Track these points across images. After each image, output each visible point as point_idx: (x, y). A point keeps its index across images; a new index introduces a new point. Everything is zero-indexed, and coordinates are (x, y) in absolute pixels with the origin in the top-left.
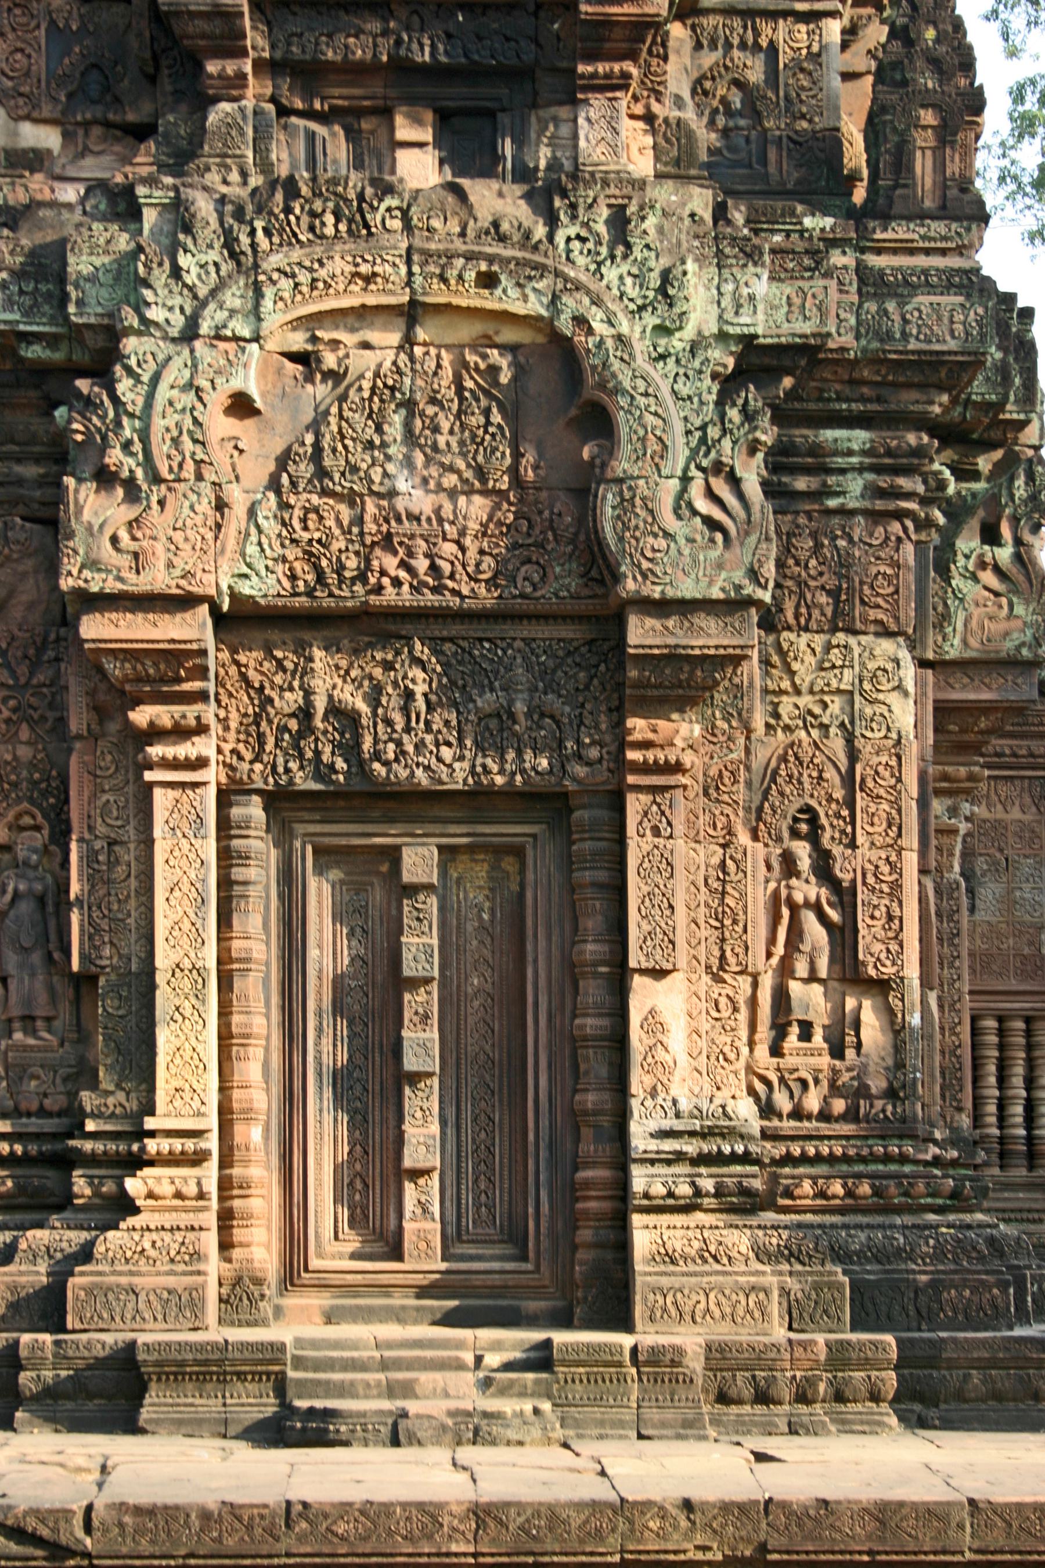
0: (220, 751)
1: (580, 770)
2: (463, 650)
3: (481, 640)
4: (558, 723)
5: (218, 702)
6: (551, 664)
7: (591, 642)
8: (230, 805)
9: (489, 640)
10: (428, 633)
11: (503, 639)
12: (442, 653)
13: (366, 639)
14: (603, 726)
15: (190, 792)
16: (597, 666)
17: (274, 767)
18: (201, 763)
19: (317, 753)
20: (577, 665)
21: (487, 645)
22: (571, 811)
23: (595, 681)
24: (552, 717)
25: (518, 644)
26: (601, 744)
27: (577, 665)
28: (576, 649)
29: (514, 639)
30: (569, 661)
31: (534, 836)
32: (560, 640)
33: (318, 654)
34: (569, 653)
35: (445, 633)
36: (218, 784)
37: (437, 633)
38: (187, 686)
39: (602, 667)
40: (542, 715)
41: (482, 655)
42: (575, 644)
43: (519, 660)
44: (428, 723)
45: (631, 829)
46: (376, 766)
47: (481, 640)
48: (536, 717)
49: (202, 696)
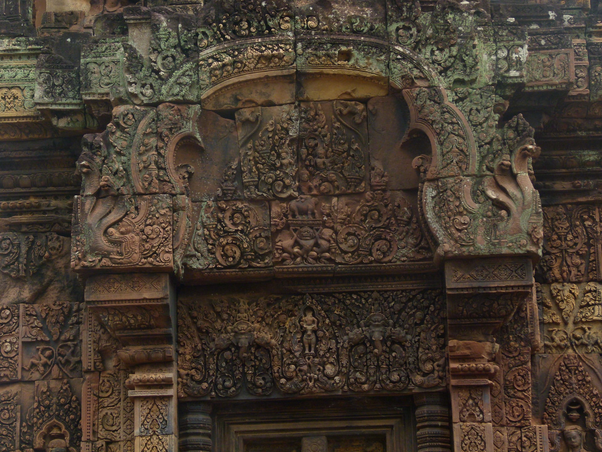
0: (179, 375)
1: (419, 378)
2: (339, 300)
3: (351, 293)
4: (403, 346)
5: (178, 342)
6: (398, 307)
7: (423, 292)
8: (187, 412)
9: (356, 293)
10: (316, 290)
11: (365, 292)
12: (325, 303)
13: (275, 296)
14: (434, 347)
15: (158, 403)
16: (428, 307)
17: (216, 384)
18: (167, 384)
19: (244, 374)
20: (415, 307)
21: (355, 297)
22: (416, 408)
23: (427, 317)
24: (400, 343)
25: (375, 295)
26: (432, 360)
27: (415, 307)
28: (414, 296)
29: (372, 292)
30: (410, 304)
31: (391, 427)
32: (403, 291)
33: (243, 306)
34: (410, 300)
35: (326, 290)
36: (179, 398)
37: (321, 290)
38: (156, 332)
39: (432, 308)
40: (393, 342)
41: (352, 304)
42: (413, 293)
43: (377, 306)
44: (316, 350)
45: (455, 417)
46: (283, 381)
47: (351, 293)
48: (389, 343)
49: (167, 339)
